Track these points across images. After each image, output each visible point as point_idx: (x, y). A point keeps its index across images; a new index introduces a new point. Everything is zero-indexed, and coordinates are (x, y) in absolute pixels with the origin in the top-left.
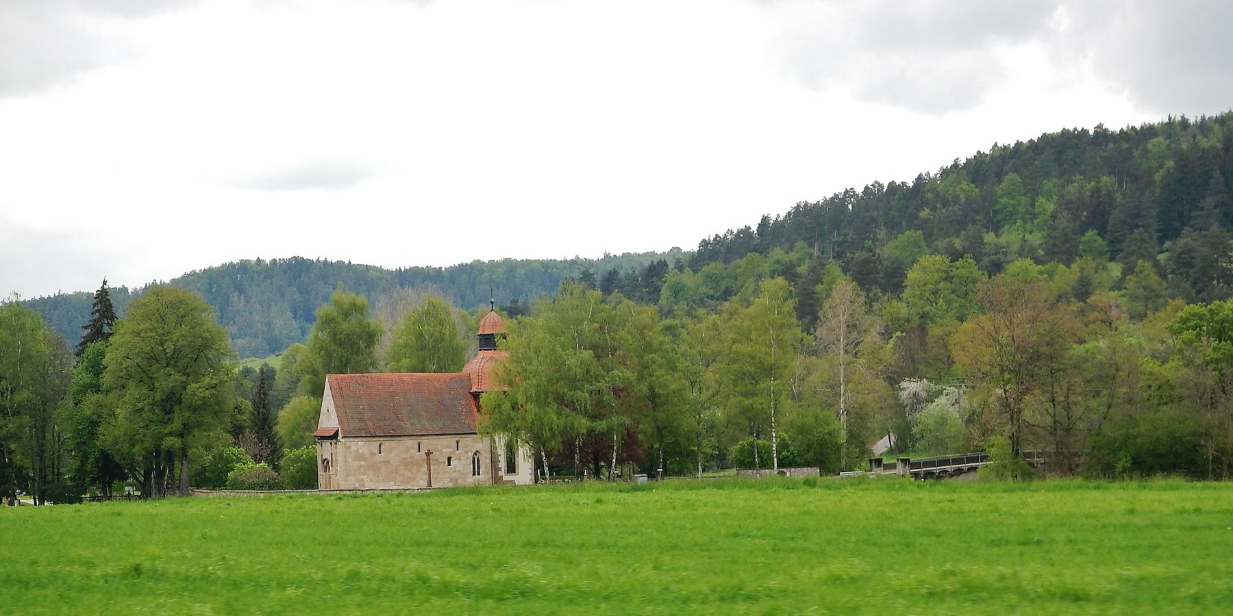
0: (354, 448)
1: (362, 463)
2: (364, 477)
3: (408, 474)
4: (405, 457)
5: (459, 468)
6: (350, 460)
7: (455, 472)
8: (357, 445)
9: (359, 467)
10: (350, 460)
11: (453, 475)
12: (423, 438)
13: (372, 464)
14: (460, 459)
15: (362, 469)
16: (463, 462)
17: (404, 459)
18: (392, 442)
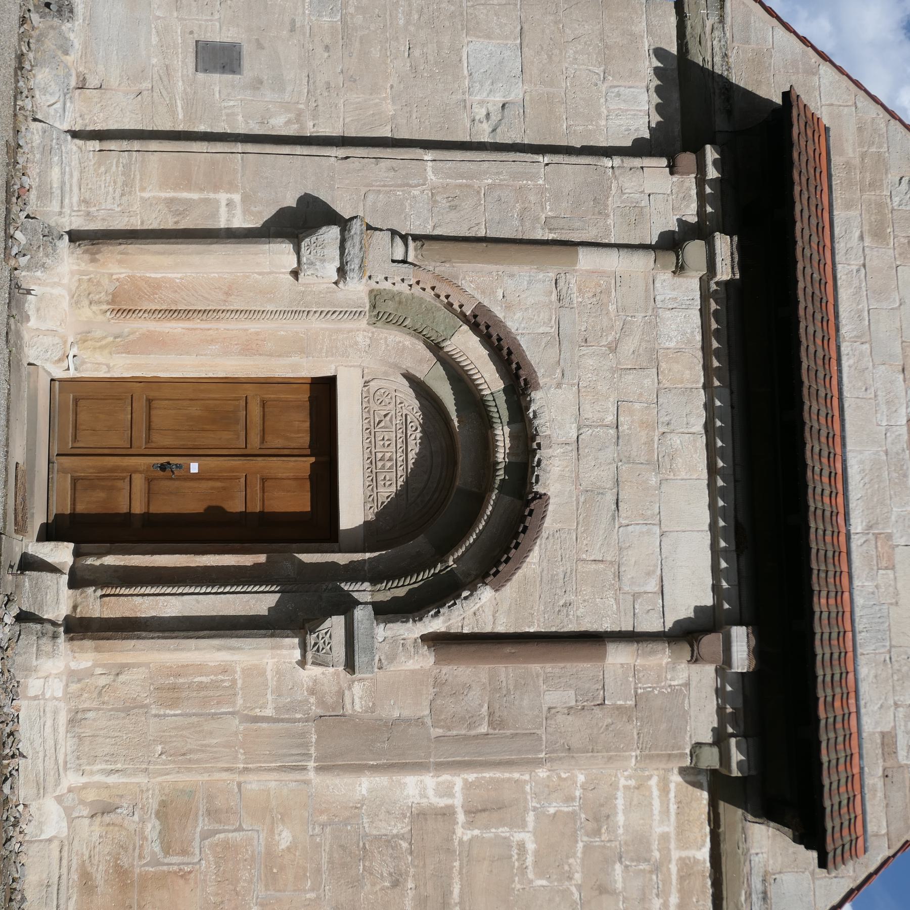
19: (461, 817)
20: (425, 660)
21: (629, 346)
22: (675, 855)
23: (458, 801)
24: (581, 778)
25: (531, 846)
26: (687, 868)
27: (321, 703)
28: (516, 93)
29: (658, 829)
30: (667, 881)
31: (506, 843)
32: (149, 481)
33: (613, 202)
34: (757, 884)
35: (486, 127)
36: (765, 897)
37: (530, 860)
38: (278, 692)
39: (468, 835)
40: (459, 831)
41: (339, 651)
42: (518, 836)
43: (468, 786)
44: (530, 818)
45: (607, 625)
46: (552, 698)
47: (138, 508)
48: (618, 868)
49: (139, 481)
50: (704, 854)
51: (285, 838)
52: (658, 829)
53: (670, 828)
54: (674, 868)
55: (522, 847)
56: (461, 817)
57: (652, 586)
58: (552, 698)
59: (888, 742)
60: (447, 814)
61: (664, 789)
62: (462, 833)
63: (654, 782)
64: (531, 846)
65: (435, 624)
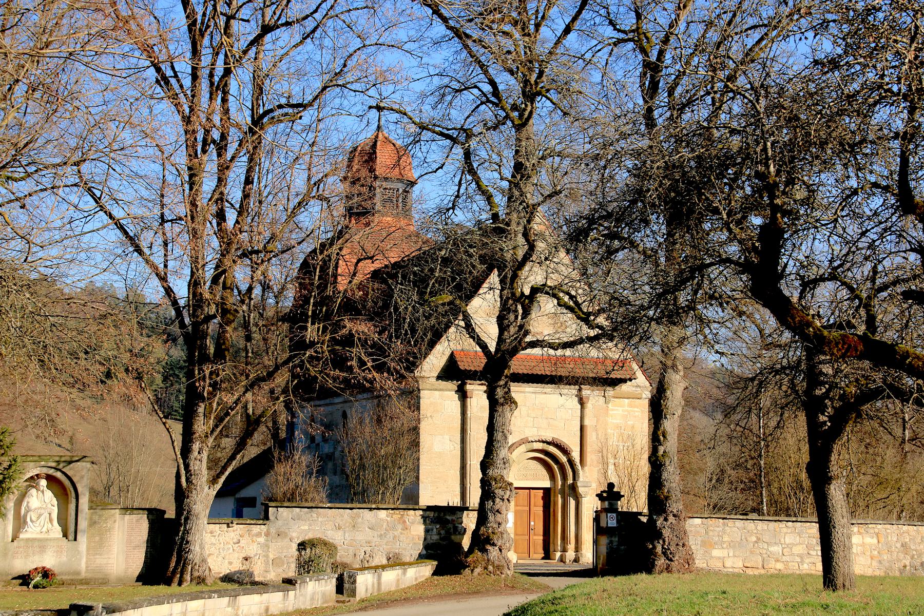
20: (586, 468)
22: (626, 408)
26: (630, 405)
28: (447, 437)
29: (621, 412)
32: (535, 535)
33: (479, 414)
35: (456, 445)
41: (586, 489)
45: (579, 423)
47: (542, 538)
49: (535, 537)
50: (626, 400)
53: (621, 409)
61: (613, 410)
65: (580, 468)
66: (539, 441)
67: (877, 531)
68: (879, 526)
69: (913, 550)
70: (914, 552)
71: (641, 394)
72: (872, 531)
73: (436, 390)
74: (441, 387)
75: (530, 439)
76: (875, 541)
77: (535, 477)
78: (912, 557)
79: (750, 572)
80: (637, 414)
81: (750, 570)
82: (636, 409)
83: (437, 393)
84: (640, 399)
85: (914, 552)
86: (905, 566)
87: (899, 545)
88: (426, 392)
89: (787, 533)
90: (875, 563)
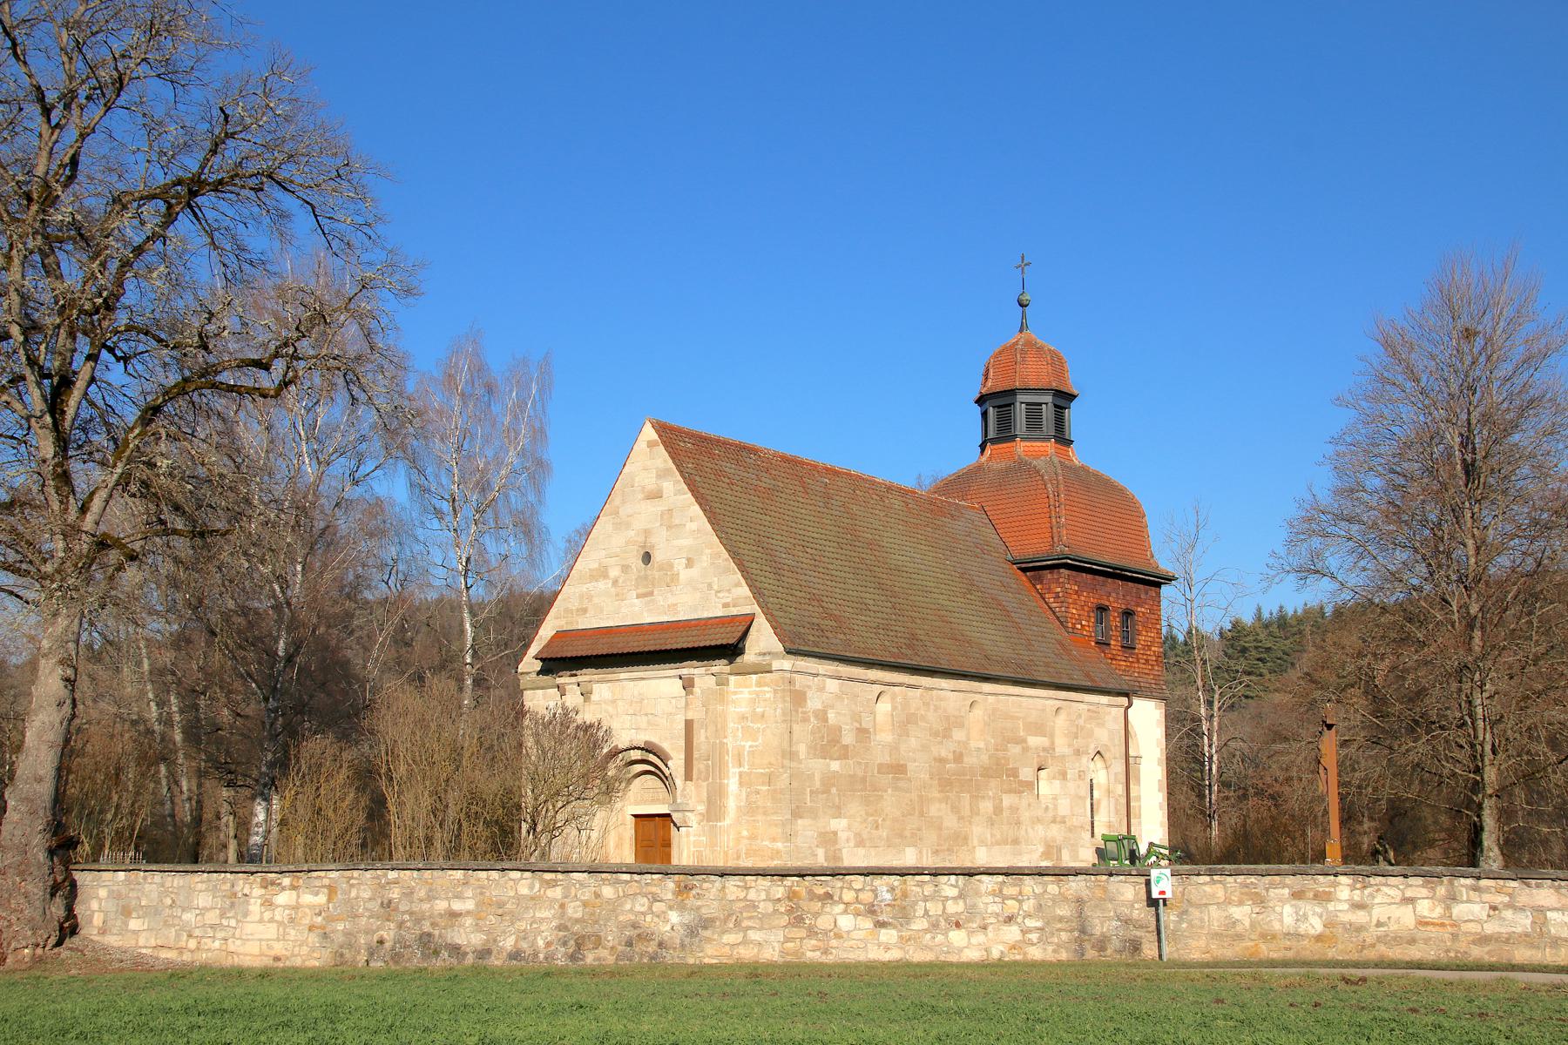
0: (814, 703)
1: (835, 766)
2: (838, 824)
3: (951, 822)
4: (943, 754)
5: (1064, 808)
6: (802, 749)
7: (1054, 821)
8: (822, 689)
9: (829, 781)
10: (802, 749)
11: (1055, 832)
12: (987, 687)
13: (860, 773)
14: (1063, 775)
15: (834, 790)
16: (1071, 785)
17: (942, 761)
18: (911, 692)
19: (741, 769)
21: (610, 709)
22: (754, 688)
23: (737, 770)
24: (732, 725)
25: (750, 743)
26: (759, 684)
27: (702, 821)
29: (747, 696)
30: (761, 691)
31: (749, 752)
34: (761, 658)
36: (765, 654)
37: (754, 744)
38: (699, 836)
39: (747, 767)
40: (746, 770)
42: (747, 748)
43: (733, 767)
44: (743, 743)
46: (703, 738)
48: (758, 710)
50: (754, 676)
51: (745, 833)
52: (747, 696)
53: (746, 690)
54: (758, 689)
55: (750, 747)
56: (741, 769)
57: (674, 701)
58: (703, 738)
59: (726, 605)
60: (741, 775)
61: (735, 693)
62: (746, 769)
63: (734, 697)
64: (750, 743)
66: (639, 748)
67: (326, 882)
68: (333, 875)
69: (404, 913)
70: (407, 917)
71: (770, 665)
72: (318, 883)
73: (538, 688)
74: (542, 684)
75: (621, 746)
76: (322, 899)
77: (654, 801)
78: (401, 925)
79: (164, 954)
80: (768, 695)
81: (165, 950)
82: (766, 689)
83: (540, 692)
84: (771, 672)
85: (407, 917)
86: (381, 942)
87: (375, 906)
88: (528, 692)
89: (201, 891)
90: (313, 939)
